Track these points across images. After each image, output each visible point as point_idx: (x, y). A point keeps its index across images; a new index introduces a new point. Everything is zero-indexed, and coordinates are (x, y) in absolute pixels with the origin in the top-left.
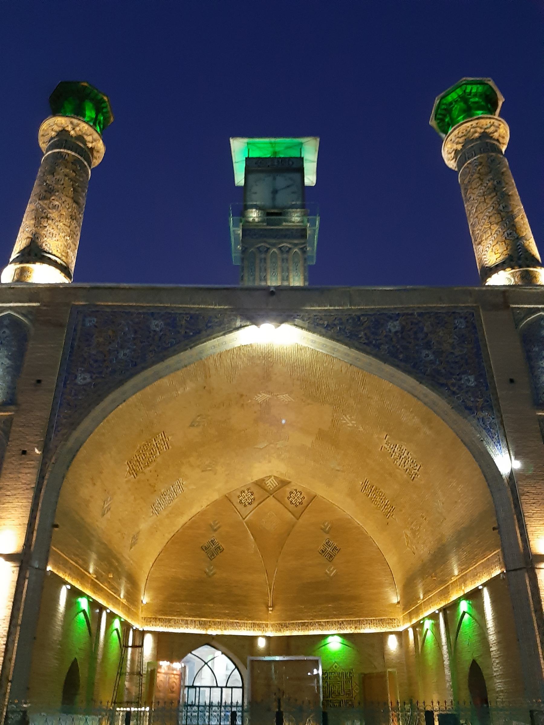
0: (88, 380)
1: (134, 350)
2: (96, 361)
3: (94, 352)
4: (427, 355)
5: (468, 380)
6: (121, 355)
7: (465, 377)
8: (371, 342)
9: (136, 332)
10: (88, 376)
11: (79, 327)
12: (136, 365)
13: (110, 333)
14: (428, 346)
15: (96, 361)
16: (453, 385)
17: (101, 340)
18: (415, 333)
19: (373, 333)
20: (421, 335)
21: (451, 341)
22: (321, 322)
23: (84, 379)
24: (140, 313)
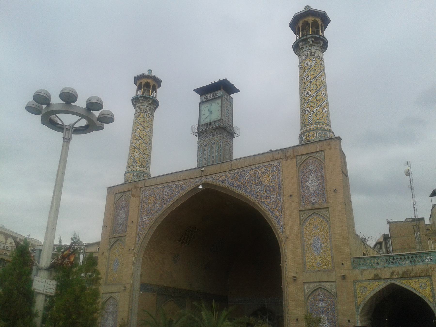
3: (148, 207)
4: (258, 188)
5: (273, 198)
6: (156, 207)
7: (272, 197)
8: (238, 186)
13: (152, 198)
15: (148, 211)
20: (257, 179)
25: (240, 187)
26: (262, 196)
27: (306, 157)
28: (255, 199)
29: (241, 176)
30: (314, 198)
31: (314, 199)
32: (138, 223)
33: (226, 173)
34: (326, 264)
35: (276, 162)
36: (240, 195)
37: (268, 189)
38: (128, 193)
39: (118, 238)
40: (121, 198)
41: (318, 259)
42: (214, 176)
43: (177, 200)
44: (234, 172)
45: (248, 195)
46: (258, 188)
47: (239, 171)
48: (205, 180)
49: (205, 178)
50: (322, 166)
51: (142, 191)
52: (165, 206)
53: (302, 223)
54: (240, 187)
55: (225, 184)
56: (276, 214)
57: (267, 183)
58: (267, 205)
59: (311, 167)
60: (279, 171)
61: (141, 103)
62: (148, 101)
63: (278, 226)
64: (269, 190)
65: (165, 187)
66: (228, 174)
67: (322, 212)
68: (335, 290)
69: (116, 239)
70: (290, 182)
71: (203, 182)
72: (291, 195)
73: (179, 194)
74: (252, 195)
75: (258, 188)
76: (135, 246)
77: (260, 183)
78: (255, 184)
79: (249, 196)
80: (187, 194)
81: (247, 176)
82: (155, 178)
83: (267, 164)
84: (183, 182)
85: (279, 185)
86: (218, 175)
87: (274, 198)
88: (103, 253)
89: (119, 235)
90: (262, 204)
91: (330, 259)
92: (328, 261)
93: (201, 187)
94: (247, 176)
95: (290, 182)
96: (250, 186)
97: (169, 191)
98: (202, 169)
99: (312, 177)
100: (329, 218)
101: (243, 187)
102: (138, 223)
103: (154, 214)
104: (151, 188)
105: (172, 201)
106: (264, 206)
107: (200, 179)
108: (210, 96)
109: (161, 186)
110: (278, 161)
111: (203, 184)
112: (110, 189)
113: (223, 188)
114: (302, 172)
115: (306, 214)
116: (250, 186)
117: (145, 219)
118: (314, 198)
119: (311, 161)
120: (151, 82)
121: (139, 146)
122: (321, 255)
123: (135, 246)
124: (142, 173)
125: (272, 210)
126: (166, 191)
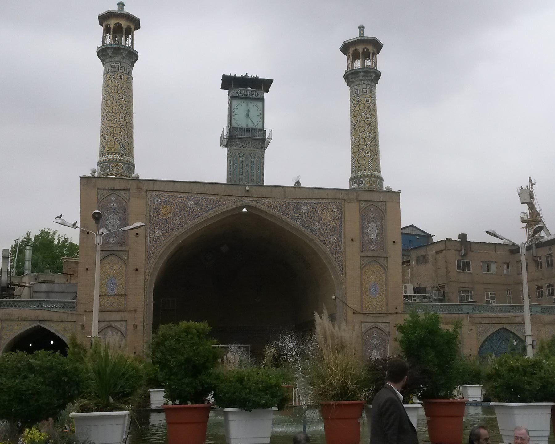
0: (161, 234)
1: (181, 218)
2: (163, 224)
4: (318, 226)
5: (334, 239)
6: (175, 221)
9: (180, 208)
10: (160, 232)
11: (152, 205)
12: (182, 226)
13: (168, 208)
14: (319, 220)
15: (163, 224)
16: (327, 241)
17: (164, 212)
18: (314, 213)
19: (295, 213)
20: (316, 215)
21: (329, 218)
22: (270, 205)
23: (159, 233)
24: (181, 197)
25: (296, 220)
26: (322, 235)
27: (370, 203)
28: (314, 236)
29: (298, 208)
30: (373, 245)
31: (373, 247)
32: (146, 237)
33: (277, 200)
34: (380, 308)
35: (338, 201)
36: (297, 230)
37: (328, 228)
38: (122, 193)
39: (112, 252)
40: (109, 197)
41: (374, 303)
43: (208, 218)
44: (288, 201)
45: (306, 230)
46: (317, 225)
48: (249, 201)
49: (248, 199)
50: (382, 217)
51: (148, 195)
53: (362, 268)
54: (296, 220)
55: (276, 212)
56: (337, 256)
57: (327, 221)
58: (327, 245)
59: (372, 215)
60: (341, 211)
61: (123, 58)
62: (132, 58)
63: (338, 267)
64: (330, 230)
65: (188, 198)
66: (282, 202)
67: (381, 261)
68: (388, 330)
69: (108, 253)
70: (352, 227)
71: (247, 203)
72: (352, 240)
73: (211, 212)
74: (311, 232)
75: (318, 226)
76: (145, 266)
77: (319, 220)
78: (314, 220)
79: (307, 232)
80: (223, 213)
81: (304, 209)
82: (172, 184)
83: (328, 201)
85: (340, 226)
86: (266, 200)
87: (335, 239)
88: (87, 269)
89: (116, 248)
90: (322, 244)
91: (384, 303)
92: (383, 305)
93: (245, 210)
95: (352, 227)
96: (309, 221)
98: (247, 188)
99: (372, 225)
100: (387, 267)
101: (299, 220)
102: (146, 237)
103: (172, 229)
104: (166, 194)
105: (202, 218)
106: (324, 245)
107: (242, 199)
108: (243, 92)
109: (182, 195)
110: (340, 201)
111: (247, 207)
112: (83, 178)
113: (272, 216)
114: (364, 218)
115: (366, 259)
116: (309, 221)
117: (158, 233)
118: (373, 245)
119: (372, 209)
120: (124, 23)
121: (126, 125)
122: (376, 299)
123: (145, 266)
124: (121, 163)
125: (333, 251)
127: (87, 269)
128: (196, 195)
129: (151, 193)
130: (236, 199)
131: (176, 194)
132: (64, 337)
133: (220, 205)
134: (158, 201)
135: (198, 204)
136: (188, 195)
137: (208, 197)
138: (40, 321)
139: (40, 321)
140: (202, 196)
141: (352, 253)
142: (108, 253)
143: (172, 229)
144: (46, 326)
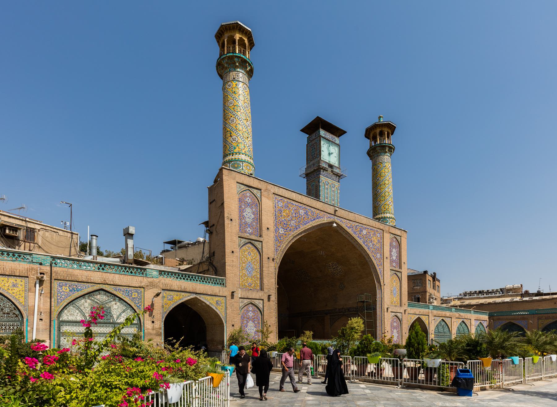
25: (361, 239)
29: (361, 231)
33: (351, 222)
42: (343, 219)
44: (357, 224)
47: (360, 225)
52: (303, 228)
55: (350, 231)
57: (375, 243)
69: (247, 241)
84: (318, 211)
86: (346, 220)
87: (379, 256)
88: (233, 252)
93: (335, 225)
94: (364, 232)
97: (305, 213)
98: (337, 209)
103: (290, 230)
104: (286, 200)
107: (332, 216)
117: (281, 231)
126: (302, 212)
127: (233, 252)
128: (305, 206)
129: (276, 196)
130: (329, 215)
131: (292, 202)
132: (217, 309)
133: (320, 217)
134: (281, 204)
135: (306, 213)
136: (300, 205)
137: (312, 209)
138: (196, 293)
139: (196, 293)
140: (308, 208)
141: (387, 265)
142: (247, 241)
143: (290, 230)
144: (202, 298)
